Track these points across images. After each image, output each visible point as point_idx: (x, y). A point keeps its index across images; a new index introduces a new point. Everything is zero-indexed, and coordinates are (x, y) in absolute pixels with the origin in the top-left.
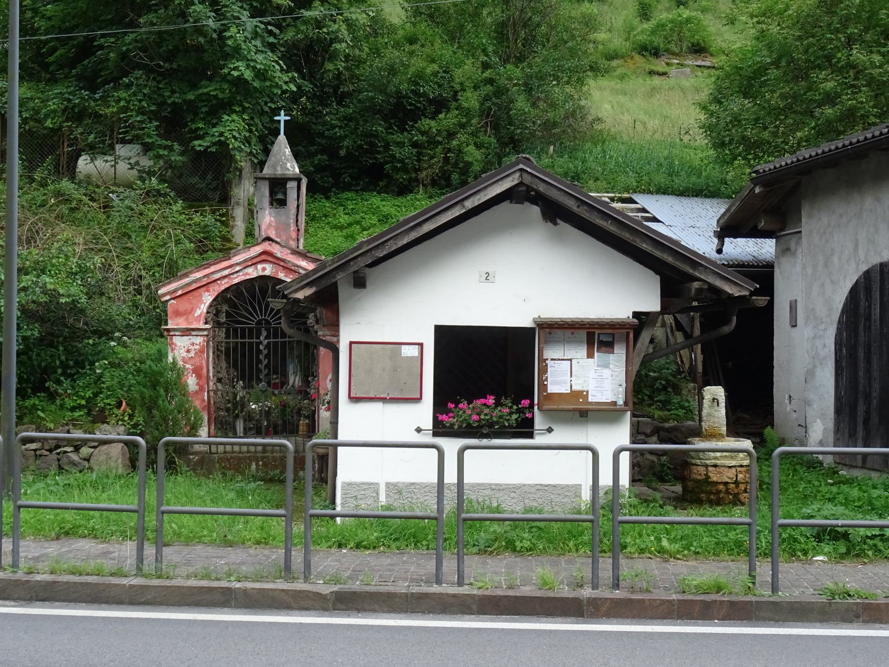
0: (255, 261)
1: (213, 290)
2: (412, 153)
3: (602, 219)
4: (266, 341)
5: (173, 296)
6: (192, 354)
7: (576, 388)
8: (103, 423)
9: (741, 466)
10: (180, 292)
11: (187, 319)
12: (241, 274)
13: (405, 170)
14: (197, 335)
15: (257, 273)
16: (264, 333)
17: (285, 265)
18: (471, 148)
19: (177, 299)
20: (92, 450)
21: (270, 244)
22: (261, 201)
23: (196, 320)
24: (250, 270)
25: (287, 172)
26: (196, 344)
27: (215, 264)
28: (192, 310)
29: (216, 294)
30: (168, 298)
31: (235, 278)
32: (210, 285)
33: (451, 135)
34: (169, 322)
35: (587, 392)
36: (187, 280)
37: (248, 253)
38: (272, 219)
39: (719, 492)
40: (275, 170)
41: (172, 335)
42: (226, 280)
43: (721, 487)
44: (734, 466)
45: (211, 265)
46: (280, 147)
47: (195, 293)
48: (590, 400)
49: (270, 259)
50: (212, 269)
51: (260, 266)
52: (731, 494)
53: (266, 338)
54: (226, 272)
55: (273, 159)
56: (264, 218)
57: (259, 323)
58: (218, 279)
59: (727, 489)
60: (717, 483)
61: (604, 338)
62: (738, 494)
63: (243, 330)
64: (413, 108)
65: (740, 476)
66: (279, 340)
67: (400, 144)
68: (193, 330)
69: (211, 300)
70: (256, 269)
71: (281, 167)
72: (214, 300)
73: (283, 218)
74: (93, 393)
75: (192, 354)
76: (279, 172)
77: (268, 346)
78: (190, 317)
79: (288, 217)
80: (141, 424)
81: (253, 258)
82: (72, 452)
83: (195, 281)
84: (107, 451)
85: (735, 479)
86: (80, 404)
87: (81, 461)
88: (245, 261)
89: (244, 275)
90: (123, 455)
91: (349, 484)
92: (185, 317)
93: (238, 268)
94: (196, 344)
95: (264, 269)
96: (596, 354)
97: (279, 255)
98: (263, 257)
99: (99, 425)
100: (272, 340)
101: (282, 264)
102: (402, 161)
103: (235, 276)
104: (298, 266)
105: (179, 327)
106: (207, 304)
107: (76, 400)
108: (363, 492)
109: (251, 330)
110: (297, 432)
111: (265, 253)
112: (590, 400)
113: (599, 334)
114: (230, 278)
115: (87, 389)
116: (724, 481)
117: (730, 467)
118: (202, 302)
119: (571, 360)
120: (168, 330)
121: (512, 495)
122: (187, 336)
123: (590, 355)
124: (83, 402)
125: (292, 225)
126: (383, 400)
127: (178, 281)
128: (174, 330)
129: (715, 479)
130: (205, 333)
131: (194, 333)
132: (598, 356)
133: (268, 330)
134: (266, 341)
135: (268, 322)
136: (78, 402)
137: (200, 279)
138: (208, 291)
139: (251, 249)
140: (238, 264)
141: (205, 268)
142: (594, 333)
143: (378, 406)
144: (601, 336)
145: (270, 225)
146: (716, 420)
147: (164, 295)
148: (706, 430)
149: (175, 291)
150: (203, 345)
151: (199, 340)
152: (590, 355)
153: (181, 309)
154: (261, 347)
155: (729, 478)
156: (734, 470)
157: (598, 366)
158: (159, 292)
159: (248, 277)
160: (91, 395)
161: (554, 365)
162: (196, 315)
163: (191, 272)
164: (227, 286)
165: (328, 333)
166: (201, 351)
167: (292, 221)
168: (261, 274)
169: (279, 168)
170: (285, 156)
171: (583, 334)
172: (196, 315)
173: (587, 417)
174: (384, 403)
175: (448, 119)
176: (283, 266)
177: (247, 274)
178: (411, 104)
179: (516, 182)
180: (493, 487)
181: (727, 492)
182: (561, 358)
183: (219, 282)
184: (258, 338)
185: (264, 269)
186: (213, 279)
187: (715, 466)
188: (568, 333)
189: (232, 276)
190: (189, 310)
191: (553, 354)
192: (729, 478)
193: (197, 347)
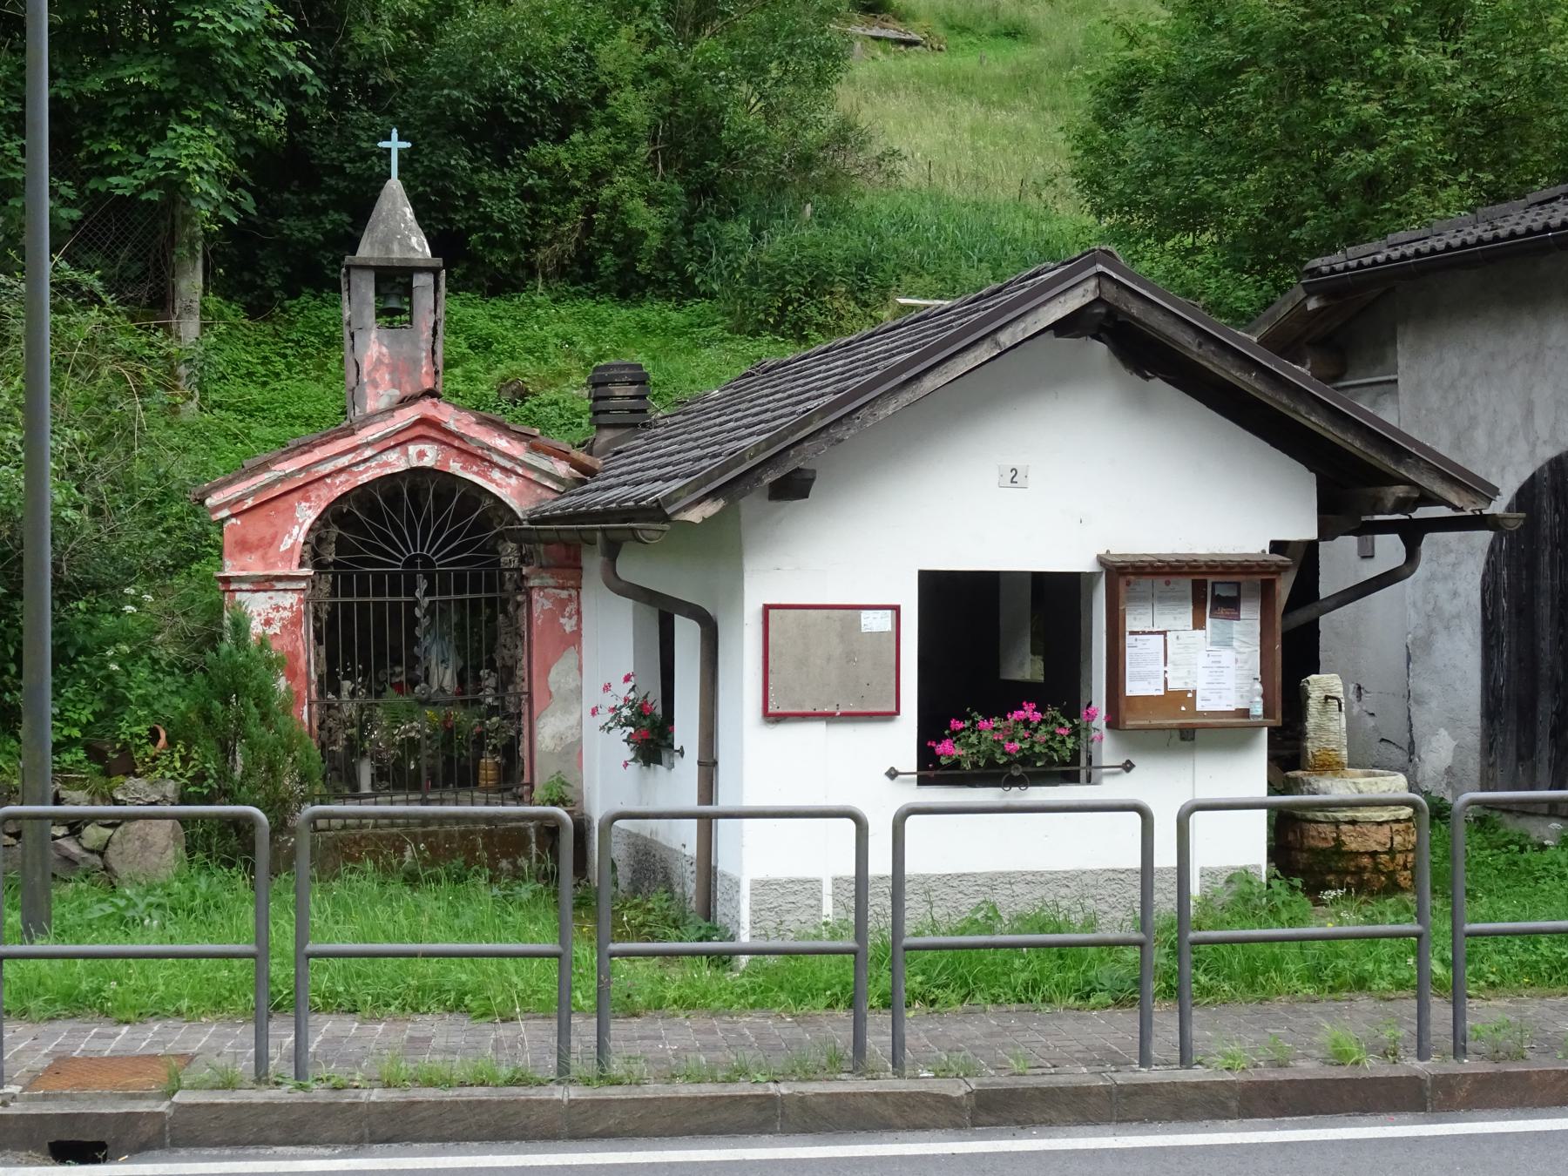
0: (402, 438)
1: (318, 496)
2: (522, 210)
3: (1240, 369)
4: (427, 600)
5: (236, 510)
6: (275, 629)
7: (1174, 685)
8: (127, 774)
9: (1397, 821)
10: (250, 502)
11: (264, 558)
12: (373, 464)
13: (507, 245)
14: (285, 590)
15: (408, 461)
16: (423, 585)
17: (463, 446)
18: (639, 203)
19: (244, 517)
20: (109, 832)
21: (435, 405)
22: (360, 314)
23: (282, 559)
24: (392, 456)
25: (412, 255)
26: (285, 609)
27: (323, 444)
28: (274, 540)
29: (324, 505)
30: (225, 513)
31: (361, 473)
32: (310, 487)
33: (599, 176)
34: (228, 562)
35: (1194, 692)
36: (265, 477)
37: (388, 422)
38: (384, 350)
39: (1362, 869)
40: (388, 250)
41: (233, 591)
42: (343, 477)
43: (1366, 861)
44: (1387, 822)
45: (315, 446)
46: (394, 203)
47: (280, 504)
48: (1199, 708)
49: (433, 433)
50: (318, 454)
51: (413, 449)
52: (1383, 873)
53: (428, 593)
54: (344, 461)
55: (382, 227)
56: (367, 346)
57: (410, 562)
59: (1376, 864)
60: (1358, 854)
61: (1222, 592)
62: (1394, 872)
63: (379, 578)
64: (521, 120)
65: (1398, 839)
66: (483, 595)
67: (498, 193)
68: (279, 578)
69: (314, 517)
70: (406, 454)
71: (400, 244)
72: (319, 518)
73: (406, 348)
74: (93, 713)
75: (275, 629)
76: (397, 254)
78: (271, 552)
79: (415, 345)
80: (212, 777)
81: (399, 432)
82: (64, 836)
83: (281, 480)
84: (141, 833)
85: (1388, 846)
86: (69, 737)
87: (86, 855)
88: (384, 438)
90: (175, 839)
91: (765, 884)
92: (260, 552)
93: (368, 453)
94: (285, 609)
95: (421, 454)
96: (1209, 621)
97: (452, 426)
98: (420, 430)
99: (121, 778)
100: (437, 598)
101: (457, 443)
102: (503, 227)
103: (361, 468)
104: (489, 449)
105: (251, 573)
106: (306, 526)
107: (62, 729)
108: (792, 899)
109: (394, 577)
110: (476, 783)
112: (1199, 708)
113: (1214, 584)
114: (352, 473)
115: (80, 706)
116: (1370, 850)
117: (1380, 824)
118: (293, 521)
119: (1164, 633)
120: (227, 580)
121: (1063, 891)
122: (265, 591)
123: (1199, 624)
124: (76, 733)
125: (424, 362)
126: (828, 717)
128: (240, 579)
129: (1354, 846)
130: (303, 585)
131: (279, 586)
132: (1213, 626)
133: (429, 577)
134: (427, 600)
135: (427, 562)
136: (66, 732)
137: (292, 474)
138: (307, 499)
139: (396, 414)
140: (368, 444)
141: (303, 453)
142: (1205, 582)
143: (818, 729)
144: (1217, 586)
145: (379, 361)
146: (1332, 736)
148: (1314, 756)
149: (240, 500)
150: (299, 610)
151: (290, 600)
152: (1199, 624)
153: (252, 537)
154: (418, 613)
155: (1379, 843)
156: (1386, 828)
157: (1212, 643)
158: (208, 502)
159: (389, 471)
160: (92, 719)
161: (1135, 644)
162: (282, 548)
163: (274, 461)
164: (346, 488)
165: (551, 582)
166: (295, 622)
167: (424, 354)
168: (415, 463)
169: (396, 247)
170: (405, 222)
171: (1185, 585)
172: (282, 548)
173: (1193, 739)
174: (828, 723)
175: (588, 145)
177: (387, 464)
178: (517, 113)
179: (1090, 298)
180: (1029, 878)
181: (1377, 870)
182: (1147, 630)
183: (328, 481)
184: (411, 591)
185: (421, 454)
186: (317, 475)
187: (1353, 822)
188: (1160, 581)
189: (355, 469)
190: (268, 537)
191: (1135, 623)
192: (1379, 843)
193: (287, 614)
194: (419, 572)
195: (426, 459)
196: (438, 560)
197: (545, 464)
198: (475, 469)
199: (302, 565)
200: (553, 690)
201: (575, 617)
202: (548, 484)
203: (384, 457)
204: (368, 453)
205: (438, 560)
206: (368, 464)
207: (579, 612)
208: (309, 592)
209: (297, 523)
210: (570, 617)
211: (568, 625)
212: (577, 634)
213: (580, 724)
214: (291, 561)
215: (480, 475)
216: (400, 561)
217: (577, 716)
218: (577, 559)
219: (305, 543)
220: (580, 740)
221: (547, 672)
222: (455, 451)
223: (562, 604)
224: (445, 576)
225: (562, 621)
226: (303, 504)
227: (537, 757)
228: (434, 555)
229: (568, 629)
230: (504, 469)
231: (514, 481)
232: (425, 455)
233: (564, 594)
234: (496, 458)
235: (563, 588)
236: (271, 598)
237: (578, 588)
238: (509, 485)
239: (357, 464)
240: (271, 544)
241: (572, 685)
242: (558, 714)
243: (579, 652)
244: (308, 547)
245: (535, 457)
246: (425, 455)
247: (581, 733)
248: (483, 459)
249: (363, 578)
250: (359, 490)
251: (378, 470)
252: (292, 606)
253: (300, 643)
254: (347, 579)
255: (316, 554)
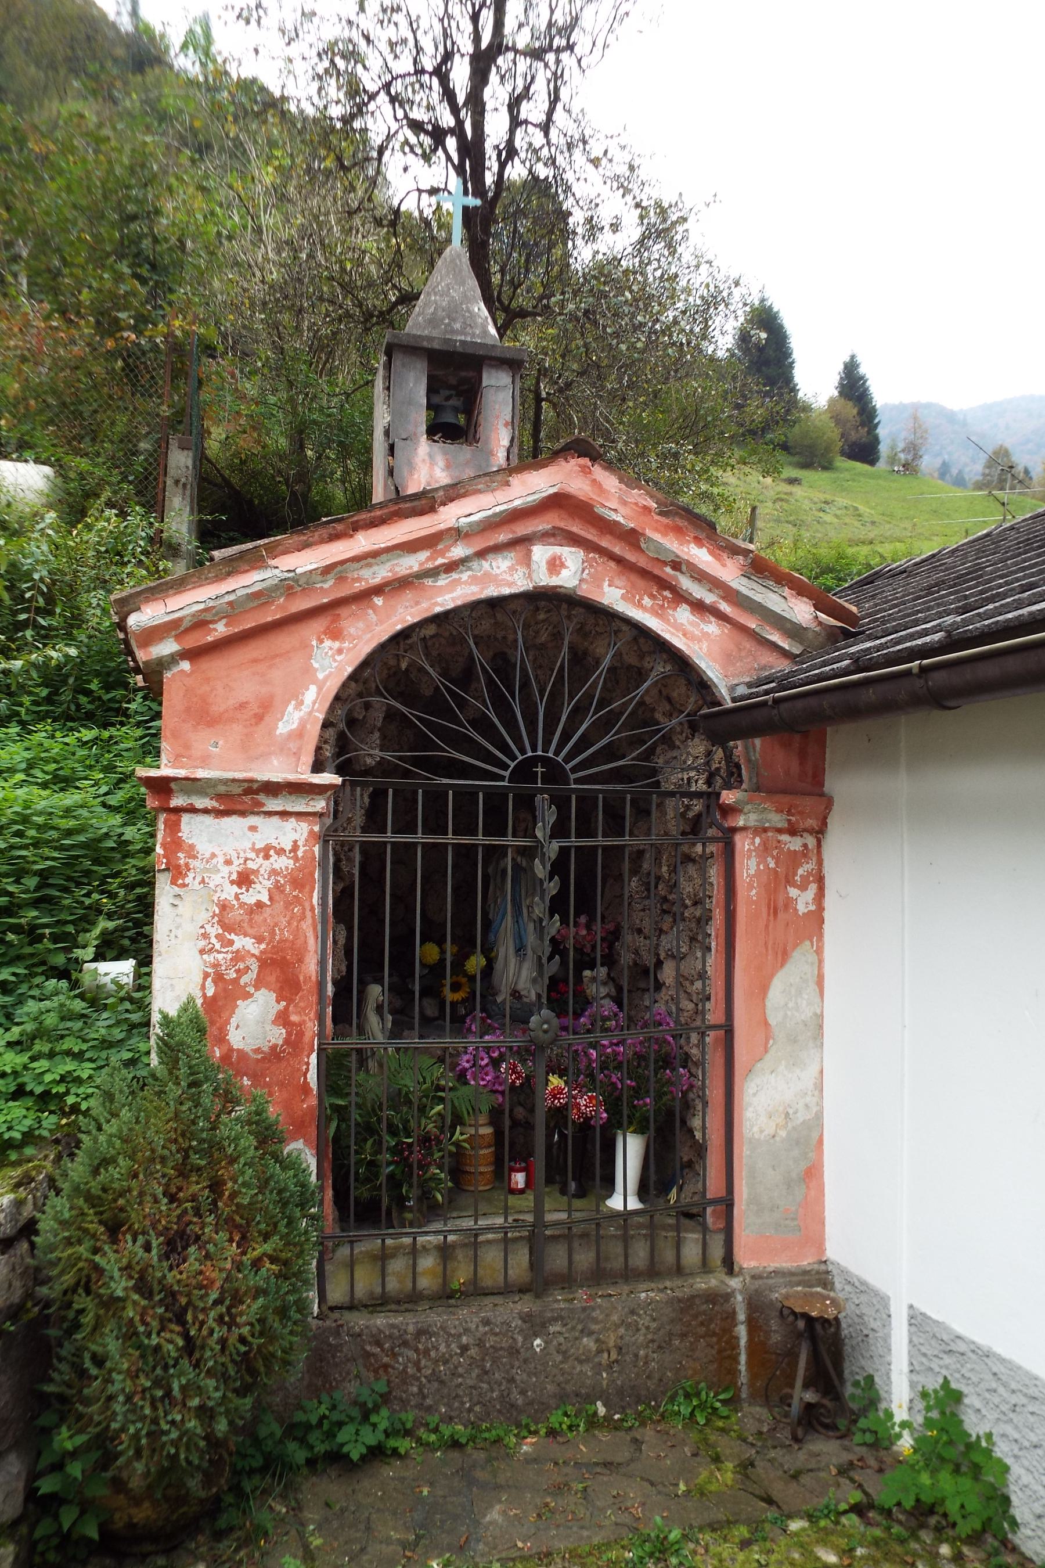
4: (555, 845)
5: (194, 640)
6: (259, 893)
10: (221, 629)
12: (465, 576)
14: (284, 814)
16: (548, 815)
17: (631, 556)
21: (585, 471)
26: (280, 852)
30: (167, 647)
31: (441, 590)
32: (344, 612)
36: (252, 580)
37: (498, 494)
41: (178, 811)
49: (576, 528)
50: (363, 542)
51: (540, 553)
53: (559, 830)
54: (412, 563)
57: (524, 772)
58: (378, 590)
63: (465, 798)
68: (272, 789)
72: (353, 677)
75: (259, 893)
77: (559, 867)
89: (474, 580)
92: (237, 730)
93: (459, 551)
94: (280, 852)
95: (555, 565)
103: (443, 581)
104: (676, 565)
109: (496, 802)
111: (558, 502)
120: (162, 786)
122: (243, 814)
127: (219, 578)
128: (192, 785)
130: (320, 805)
131: (274, 804)
133: (560, 802)
134: (555, 845)
135: (555, 774)
138: (335, 634)
139: (515, 480)
140: (457, 534)
147: (153, 634)
149: (200, 623)
150: (309, 856)
154: (540, 870)
159: (492, 591)
163: (274, 551)
165: (777, 820)
166: (299, 881)
168: (544, 579)
176: (619, 560)
177: (488, 578)
185: (555, 565)
186: (358, 586)
193: (283, 863)
194: (542, 791)
195: (565, 573)
196: (574, 770)
197: (775, 600)
198: (647, 601)
199: (318, 767)
200: (772, 1021)
201: (813, 888)
202: (775, 637)
203: (486, 565)
204: (459, 551)
205: (574, 770)
206: (454, 575)
207: (820, 880)
208: (329, 821)
209: (315, 681)
210: (803, 888)
211: (803, 900)
212: (817, 917)
213: (819, 1087)
214: (297, 755)
215: (656, 614)
216: (505, 767)
217: (813, 1070)
218: (817, 779)
219: (326, 725)
220: (819, 1116)
221: (764, 989)
222: (612, 564)
223: (795, 859)
224: (586, 801)
225: (793, 892)
226: (328, 643)
227: (743, 1153)
228: (568, 759)
229: (802, 909)
230: (699, 607)
231: (712, 628)
232: (563, 565)
233: (794, 844)
234: (686, 583)
235: (793, 831)
236: (253, 829)
237: (820, 832)
238: (706, 635)
239: (433, 573)
240: (259, 718)
241: (807, 1012)
242: (782, 1068)
243: (819, 952)
244: (331, 733)
245: (755, 586)
246: (563, 565)
247: (820, 1104)
248: (663, 584)
249: (435, 798)
250: (430, 630)
251: (474, 589)
252: (295, 847)
253: (307, 926)
254: (406, 801)
255: (342, 745)
